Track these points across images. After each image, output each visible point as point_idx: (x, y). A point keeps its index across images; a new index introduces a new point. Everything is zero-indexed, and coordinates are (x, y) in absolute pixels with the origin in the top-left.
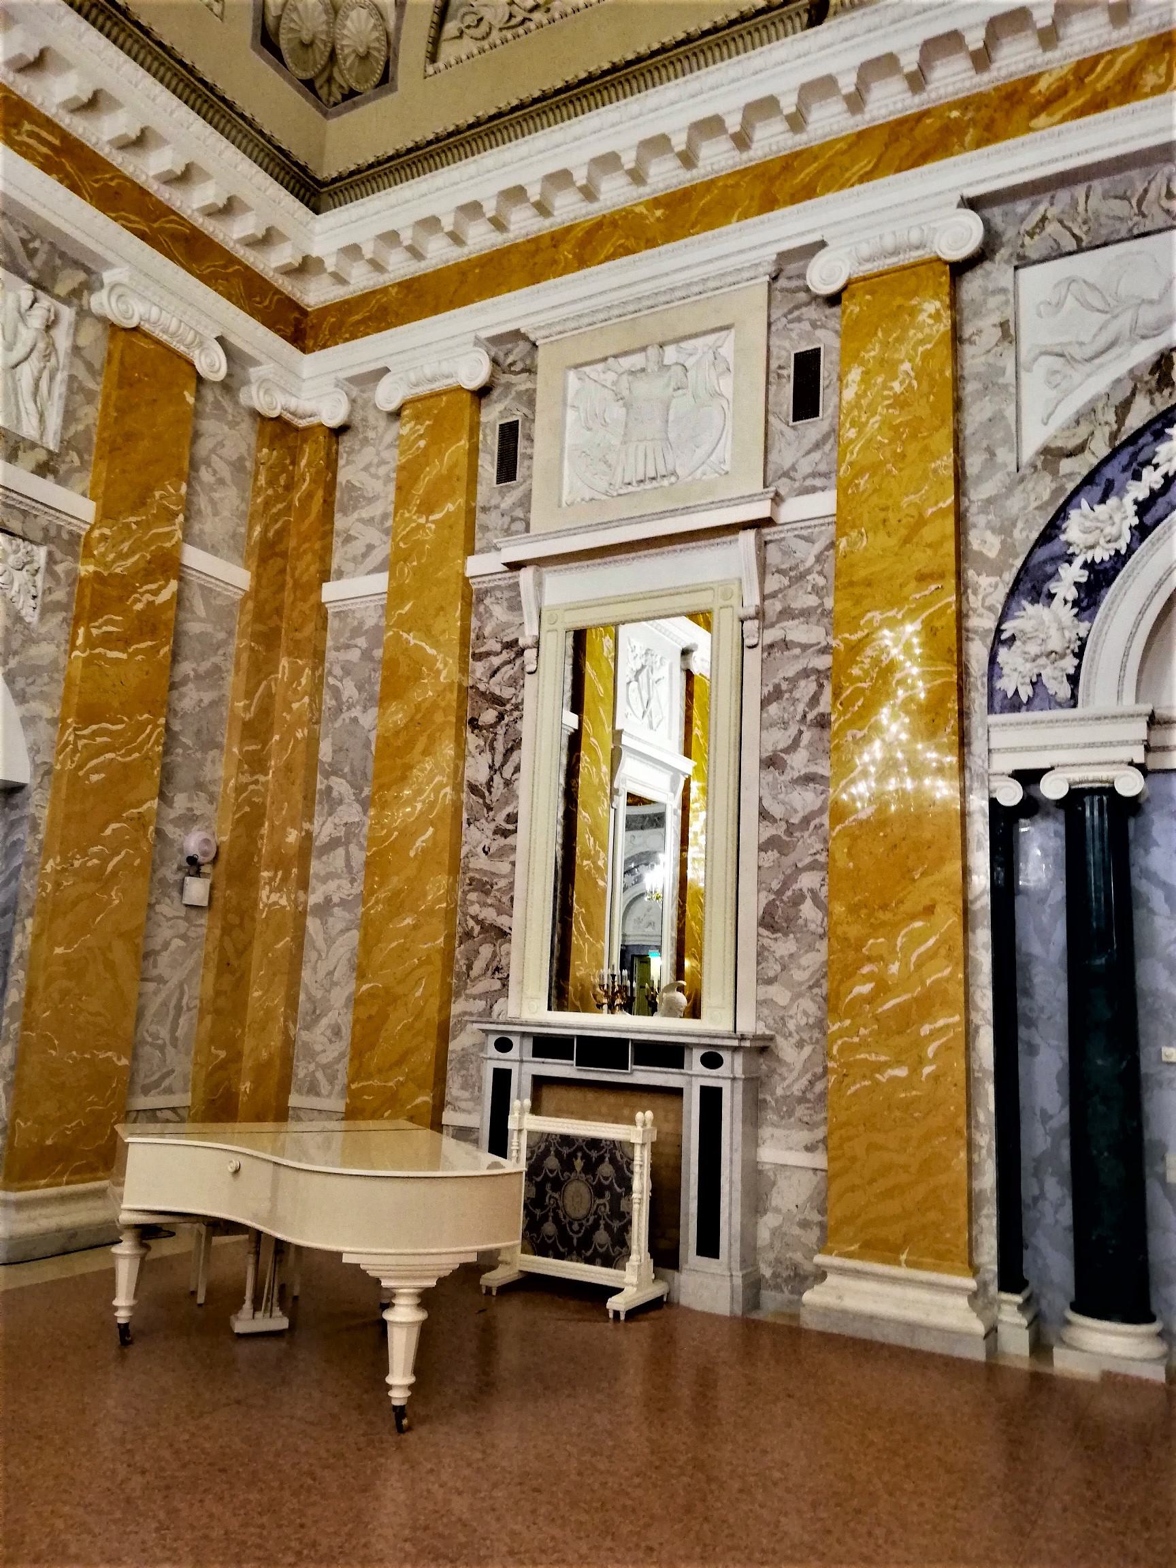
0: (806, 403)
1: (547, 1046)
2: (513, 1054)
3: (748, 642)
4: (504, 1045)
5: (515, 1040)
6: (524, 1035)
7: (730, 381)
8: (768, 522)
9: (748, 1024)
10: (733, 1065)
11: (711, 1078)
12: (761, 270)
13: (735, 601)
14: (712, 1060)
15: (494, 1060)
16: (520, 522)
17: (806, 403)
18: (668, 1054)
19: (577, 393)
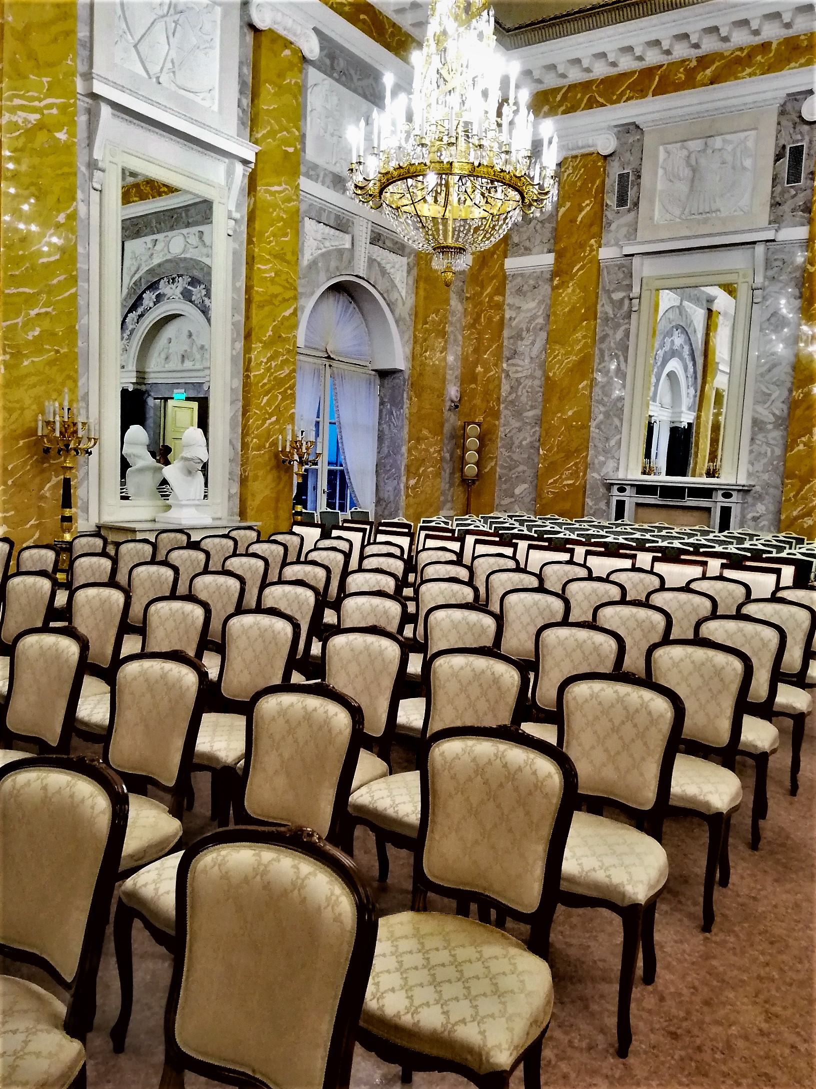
0: (794, 175)
1: (642, 489)
2: (627, 493)
3: (755, 301)
4: (622, 490)
5: (628, 488)
6: (632, 485)
7: (753, 156)
8: (774, 241)
9: (743, 480)
10: (735, 497)
11: (726, 502)
12: (777, 101)
13: (750, 280)
14: (727, 495)
15: (616, 495)
16: (633, 232)
17: (794, 175)
18: (706, 493)
19: (665, 160)
